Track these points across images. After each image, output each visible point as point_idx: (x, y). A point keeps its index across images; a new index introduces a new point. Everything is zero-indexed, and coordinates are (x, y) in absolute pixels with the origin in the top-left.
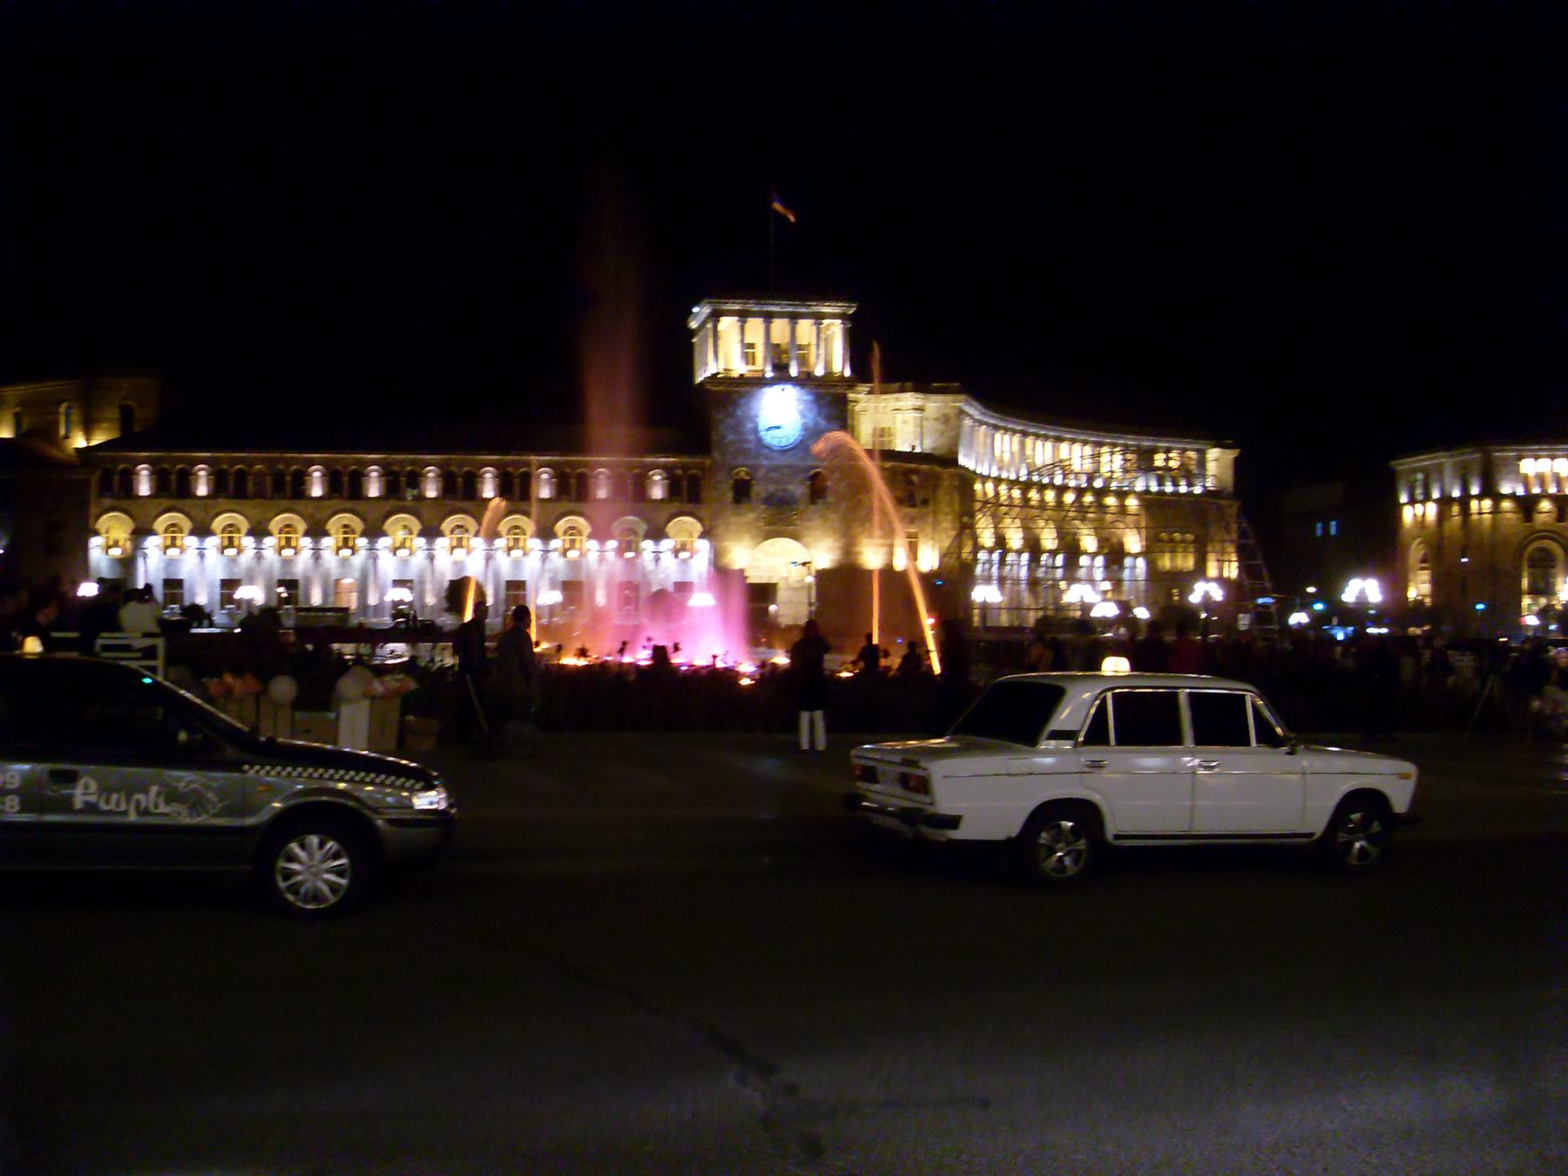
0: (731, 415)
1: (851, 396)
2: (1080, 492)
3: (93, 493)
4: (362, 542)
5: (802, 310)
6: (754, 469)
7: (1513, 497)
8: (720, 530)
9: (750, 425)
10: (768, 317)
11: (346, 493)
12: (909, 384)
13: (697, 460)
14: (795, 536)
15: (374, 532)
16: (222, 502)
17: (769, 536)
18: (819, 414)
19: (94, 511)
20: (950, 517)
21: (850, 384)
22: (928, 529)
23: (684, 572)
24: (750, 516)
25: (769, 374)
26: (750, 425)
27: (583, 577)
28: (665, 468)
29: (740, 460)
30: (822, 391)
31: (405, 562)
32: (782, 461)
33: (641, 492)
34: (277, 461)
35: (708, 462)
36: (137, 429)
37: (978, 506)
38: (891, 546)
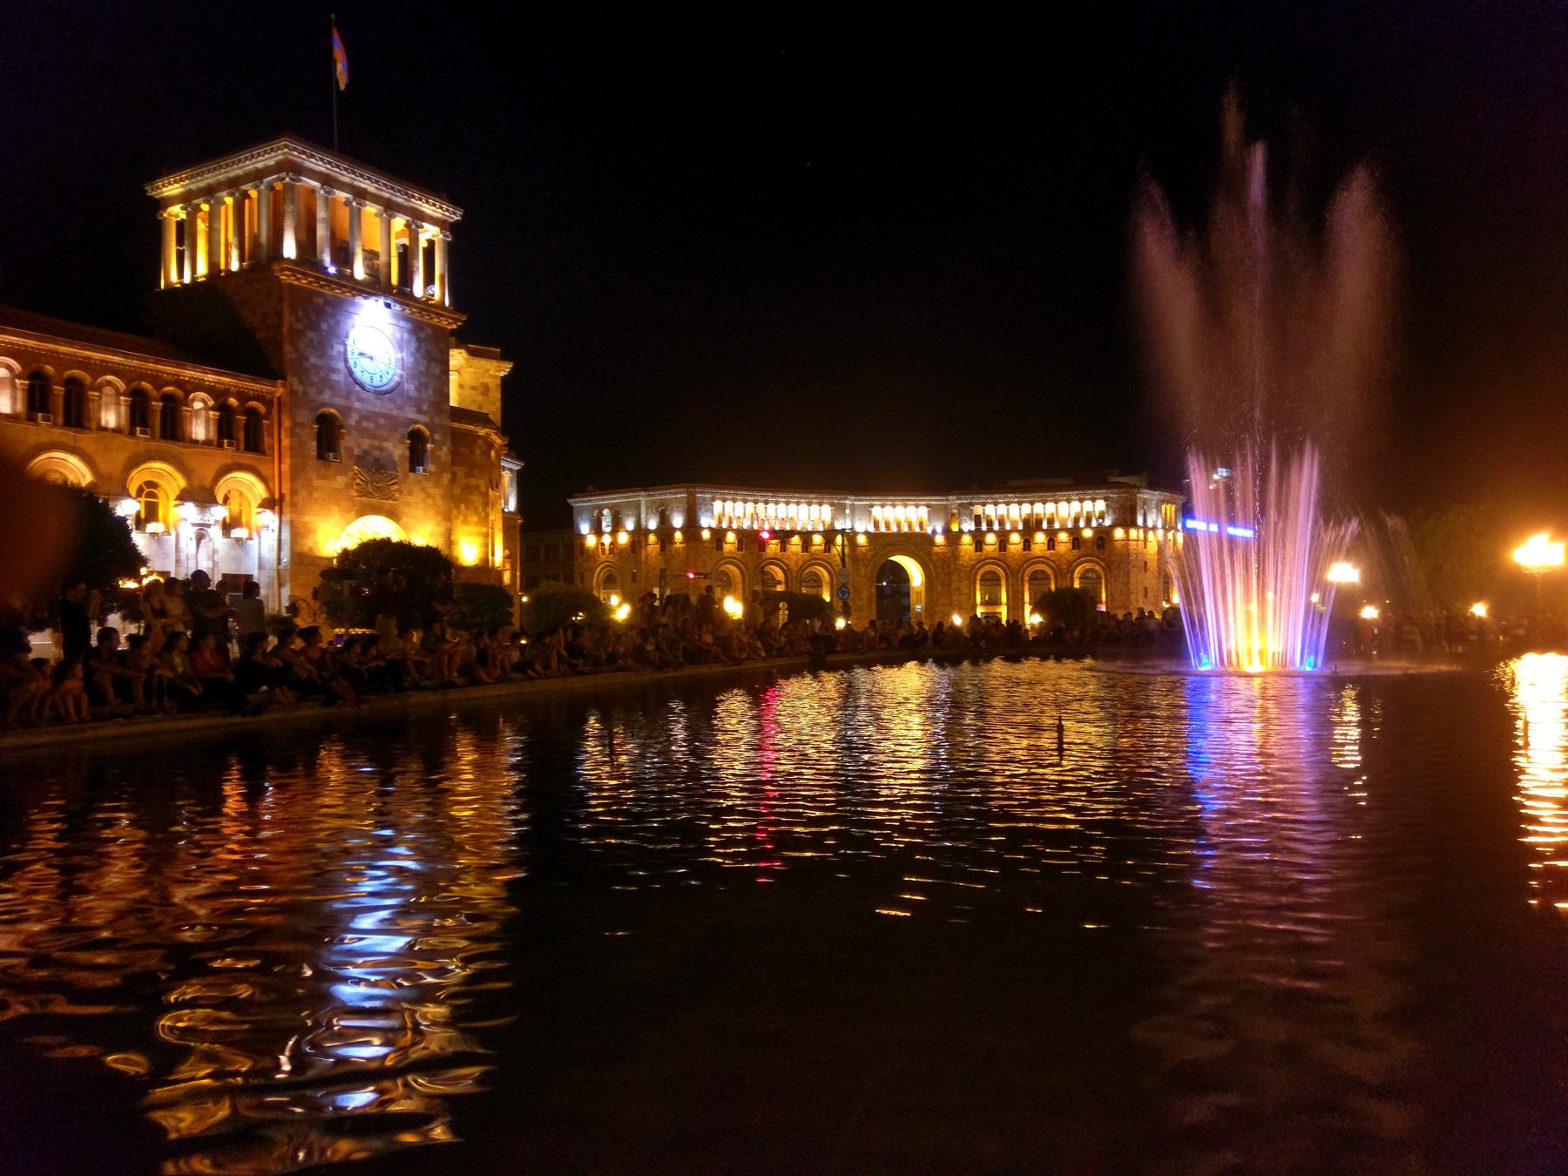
0: (313, 326)
6: (346, 411)
7: (710, 528)
8: (299, 499)
9: (341, 348)
14: (393, 515)
17: (363, 511)
18: (418, 349)
23: (238, 560)
24: (341, 481)
26: (339, 348)
28: (211, 390)
29: (326, 396)
32: (377, 406)
33: (173, 428)
35: (280, 391)
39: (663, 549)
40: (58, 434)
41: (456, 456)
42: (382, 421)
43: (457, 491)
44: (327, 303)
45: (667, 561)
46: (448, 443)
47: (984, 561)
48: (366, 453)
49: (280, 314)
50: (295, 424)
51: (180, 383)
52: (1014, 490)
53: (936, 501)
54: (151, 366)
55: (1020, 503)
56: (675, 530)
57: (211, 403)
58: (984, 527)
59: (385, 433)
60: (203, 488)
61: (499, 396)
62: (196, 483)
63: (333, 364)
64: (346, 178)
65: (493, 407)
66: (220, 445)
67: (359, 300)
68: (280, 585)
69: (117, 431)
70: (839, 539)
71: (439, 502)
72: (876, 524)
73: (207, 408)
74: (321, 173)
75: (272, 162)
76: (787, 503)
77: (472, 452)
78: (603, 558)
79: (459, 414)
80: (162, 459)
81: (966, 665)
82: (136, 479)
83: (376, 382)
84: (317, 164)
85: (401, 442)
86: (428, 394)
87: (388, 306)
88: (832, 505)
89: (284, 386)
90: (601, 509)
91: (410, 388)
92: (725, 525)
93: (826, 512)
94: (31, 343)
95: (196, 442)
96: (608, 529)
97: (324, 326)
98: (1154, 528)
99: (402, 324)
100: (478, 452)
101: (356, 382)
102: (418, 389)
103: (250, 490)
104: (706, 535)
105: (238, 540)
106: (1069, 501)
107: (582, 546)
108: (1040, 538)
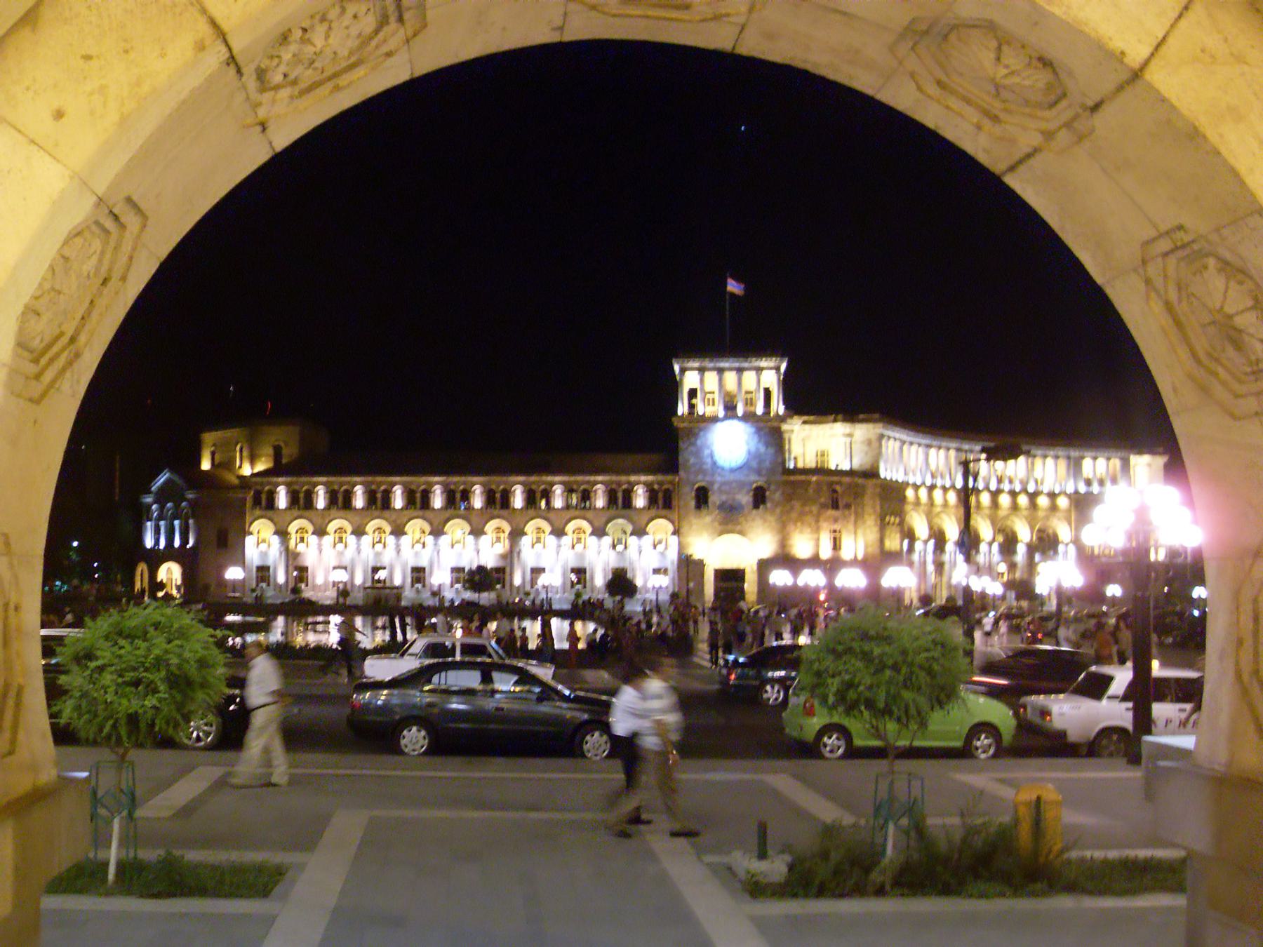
0: (694, 444)
1: (785, 427)
2: (1013, 494)
3: (249, 503)
4: (430, 539)
5: (746, 365)
6: (712, 483)
8: (684, 530)
10: (721, 371)
11: (418, 505)
12: (840, 417)
13: (670, 478)
14: (741, 533)
15: (437, 532)
16: (334, 512)
17: (721, 533)
19: (248, 519)
20: (873, 517)
21: (783, 419)
22: (851, 527)
24: (708, 519)
25: (721, 414)
26: (706, 452)
27: (586, 565)
28: (646, 484)
29: (700, 477)
30: (762, 425)
31: (460, 555)
32: (732, 477)
33: (628, 503)
34: (372, 483)
36: (284, 461)
37: (908, 508)
38: (818, 539)
80: (623, 517)
85: (748, 493)
91: (754, 464)
97: (699, 442)
100: (811, 491)
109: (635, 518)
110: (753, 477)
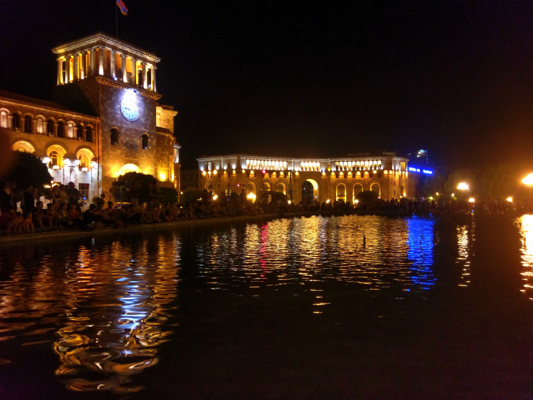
0: (110, 98)
6: (121, 128)
7: (245, 169)
8: (105, 158)
10: (126, 53)
14: (137, 164)
17: (127, 162)
18: (145, 107)
23: (84, 179)
24: (119, 152)
26: (118, 106)
28: (74, 120)
29: (114, 123)
32: (131, 126)
33: (61, 133)
35: (98, 121)
39: (229, 176)
40: (23, 135)
41: (158, 143)
42: (133, 131)
43: (159, 156)
44: (114, 90)
45: (230, 180)
46: (156, 139)
47: (339, 181)
48: (128, 142)
49: (98, 94)
50: (103, 132)
51: (64, 118)
52: (350, 157)
53: (323, 160)
54: (54, 112)
55: (352, 162)
56: (233, 170)
57: (75, 125)
58: (339, 170)
59: (134, 136)
60: (72, 154)
61: (173, 123)
62: (70, 152)
63: (116, 112)
64: (121, 47)
65: (170, 126)
66: (78, 139)
67: (125, 89)
68: (99, 187)
69: (43, 134)
70: (289, 173)
71: (153, 159)
72: (302, 168)
73: (73, 126)
74: (112, 45)
75: (95, 41)
76: (272, 161)
77: (164, 142)
78: (208, 179)
79: (160, 129)
81: (333, 217)
82: (49, 151)
83: (131, 118)
84: (110, 42)
85: (140, 138)
86: (149, 122)
87: (135, 92)
88: (287, 161)
89: (99, 119)
90: (208, 162)
91: (143, 120)
92: (250, 168)
93: (285, 164)
94: (13, 104)
95: (70, 138)
96: (210, 169)
97: (113, 98)
98: (398, 170)
99: (140, 98)
100: (166, 142)
101: (124, 118)
102: (145, 120)
103: (88, 154)
104: (244, 171)
105: (84, 172)
106: (369, 161)
107: (201, 175)
108: (358, 173)
109: (68, 145)
110: (143, 129)
